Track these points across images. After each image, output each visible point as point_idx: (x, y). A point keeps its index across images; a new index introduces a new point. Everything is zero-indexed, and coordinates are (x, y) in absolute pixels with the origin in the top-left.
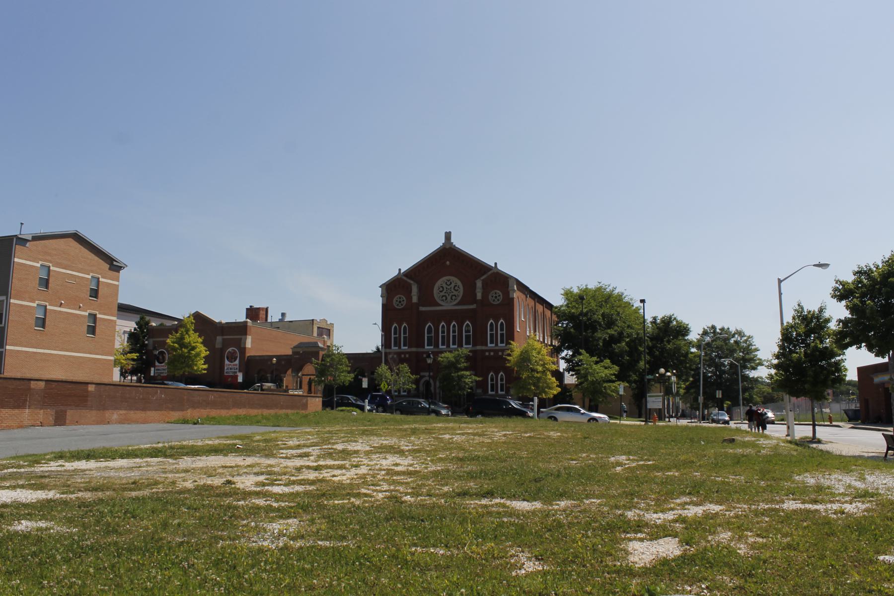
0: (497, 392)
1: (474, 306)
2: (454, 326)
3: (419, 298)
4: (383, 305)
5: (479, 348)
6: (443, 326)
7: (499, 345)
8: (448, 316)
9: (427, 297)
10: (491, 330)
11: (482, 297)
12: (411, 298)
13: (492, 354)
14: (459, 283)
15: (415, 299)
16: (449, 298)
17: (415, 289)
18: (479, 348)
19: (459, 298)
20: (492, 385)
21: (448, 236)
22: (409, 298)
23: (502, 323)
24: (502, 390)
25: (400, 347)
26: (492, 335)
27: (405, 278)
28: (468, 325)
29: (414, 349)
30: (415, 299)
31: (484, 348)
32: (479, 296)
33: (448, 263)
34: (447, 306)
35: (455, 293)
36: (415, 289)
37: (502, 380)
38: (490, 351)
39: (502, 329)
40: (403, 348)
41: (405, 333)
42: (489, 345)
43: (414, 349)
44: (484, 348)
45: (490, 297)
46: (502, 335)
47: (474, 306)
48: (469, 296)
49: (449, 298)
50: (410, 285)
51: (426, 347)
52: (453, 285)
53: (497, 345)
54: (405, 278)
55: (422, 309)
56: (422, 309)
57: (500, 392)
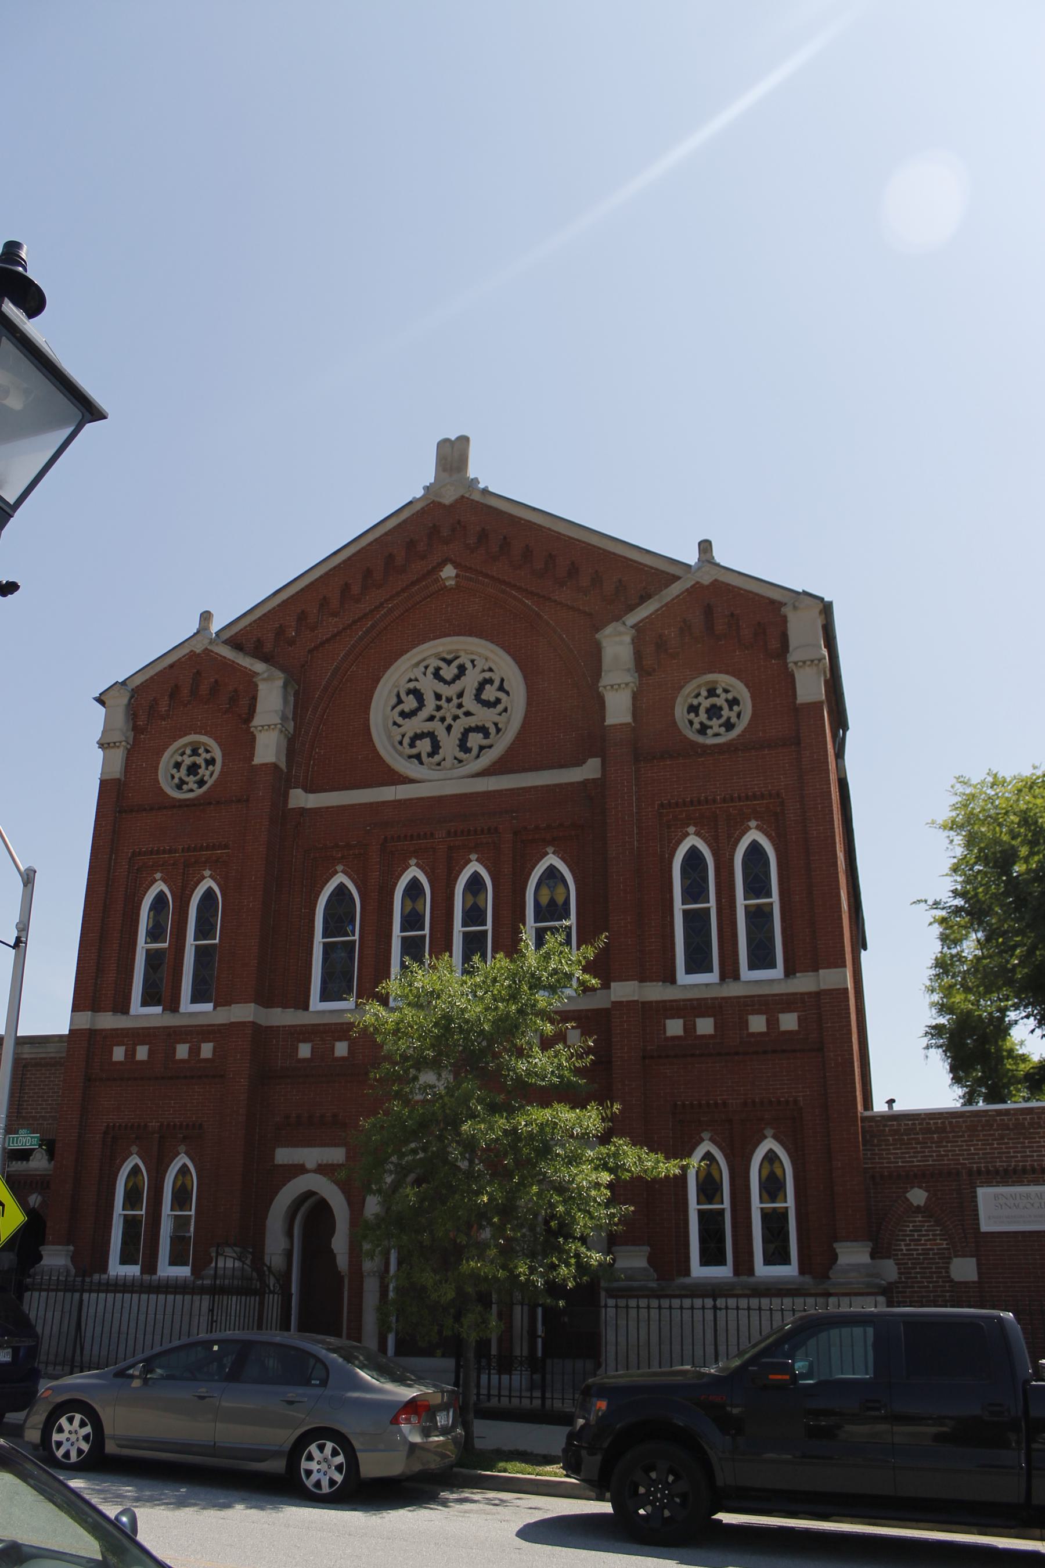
0: (744, 1265)
1: (590, 770)
2: (475, 884)
3: (292, 747)
4: (105, 786)
5: (624, 991)
6: (414, 889)
7: (746, 974)
8: (442, 831)
9: (332, 739)
10: (695, 890)
11: (636, 711)
12: (251, 741)
13: (705, 1026)
14: (506, 668)
15: (268, 748)
16: (449, 744)
17: (271, 699)
18: (624, 991)
19: (501, 745)
20: (710, 1223)
21: (453, 455)
22: (240, 742)
23: (755, 851)
24: (777, 1255)
25: (173, 1006)
26: (696, 921)
27: (226, 652)
28: (552, 873)
29: (243, 1012)
30: (268, 748)
31: (655, 992)
32: (618, 709)
33: (449, 572)
34: (433, 782)
35: (484, 716)
36: (271, 699)
37: (772, 1187)
38: (690, 1009)
39: (757, 885)
40: (186, 1005)
41: (204, 929)
42: (683, 978)
43: (243, 1012)
44: (655, 992)
45: (680, 712)
46: (759, 917)
47: (590, 770)
48: (562, 720)
49: (449, 744)
50: (250, 681)
51: (316, 1003)
52: (471, 680)
53: (730, 972)
54: (226, 652)
55: (300, 799)
56: (300, 799)
57: (762, 1270)
